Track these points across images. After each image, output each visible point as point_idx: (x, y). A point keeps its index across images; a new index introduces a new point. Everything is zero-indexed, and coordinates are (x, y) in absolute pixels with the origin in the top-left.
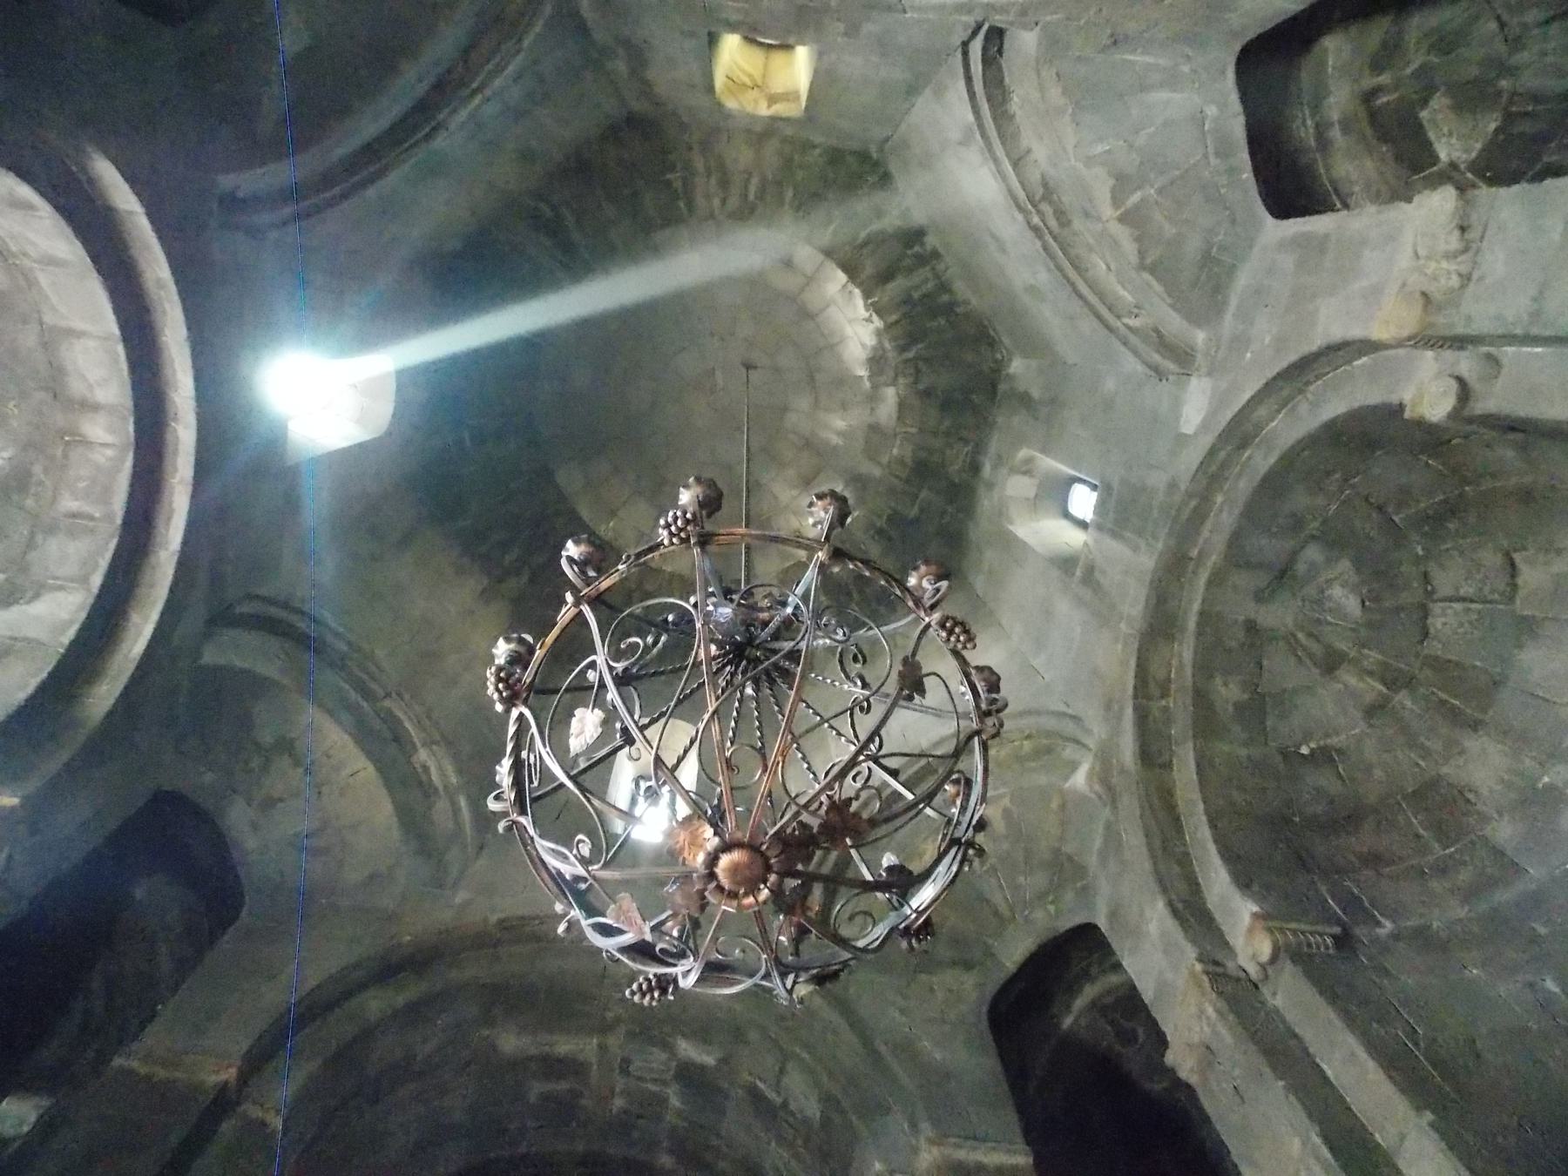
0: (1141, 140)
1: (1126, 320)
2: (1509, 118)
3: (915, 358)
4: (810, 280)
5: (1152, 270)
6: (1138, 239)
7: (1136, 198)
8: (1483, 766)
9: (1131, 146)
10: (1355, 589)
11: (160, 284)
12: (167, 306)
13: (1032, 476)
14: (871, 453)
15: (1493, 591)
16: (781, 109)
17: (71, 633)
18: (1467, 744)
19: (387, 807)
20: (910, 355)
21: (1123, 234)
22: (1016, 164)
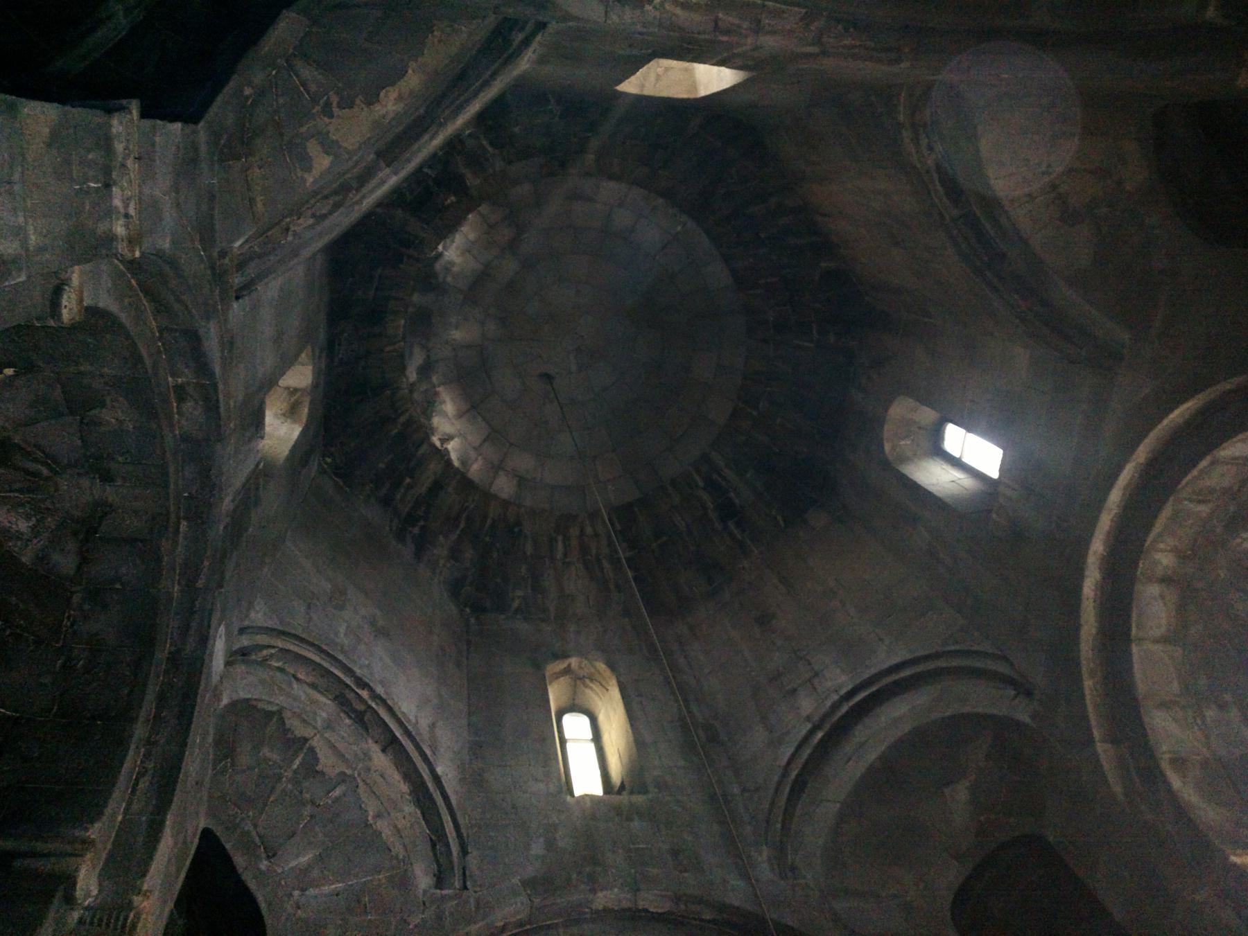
0: (307, 811)
1: (273, 651)
5: (270, 715)
9: (313, 802)
11: (1092, 674)
12: (1090, 654)
13: (287, 388)
16: (560, 666)
17: (1240, 436)
19: (984, 145)
20: (402, 419)
21: (300, 730)
22: (394, 740)
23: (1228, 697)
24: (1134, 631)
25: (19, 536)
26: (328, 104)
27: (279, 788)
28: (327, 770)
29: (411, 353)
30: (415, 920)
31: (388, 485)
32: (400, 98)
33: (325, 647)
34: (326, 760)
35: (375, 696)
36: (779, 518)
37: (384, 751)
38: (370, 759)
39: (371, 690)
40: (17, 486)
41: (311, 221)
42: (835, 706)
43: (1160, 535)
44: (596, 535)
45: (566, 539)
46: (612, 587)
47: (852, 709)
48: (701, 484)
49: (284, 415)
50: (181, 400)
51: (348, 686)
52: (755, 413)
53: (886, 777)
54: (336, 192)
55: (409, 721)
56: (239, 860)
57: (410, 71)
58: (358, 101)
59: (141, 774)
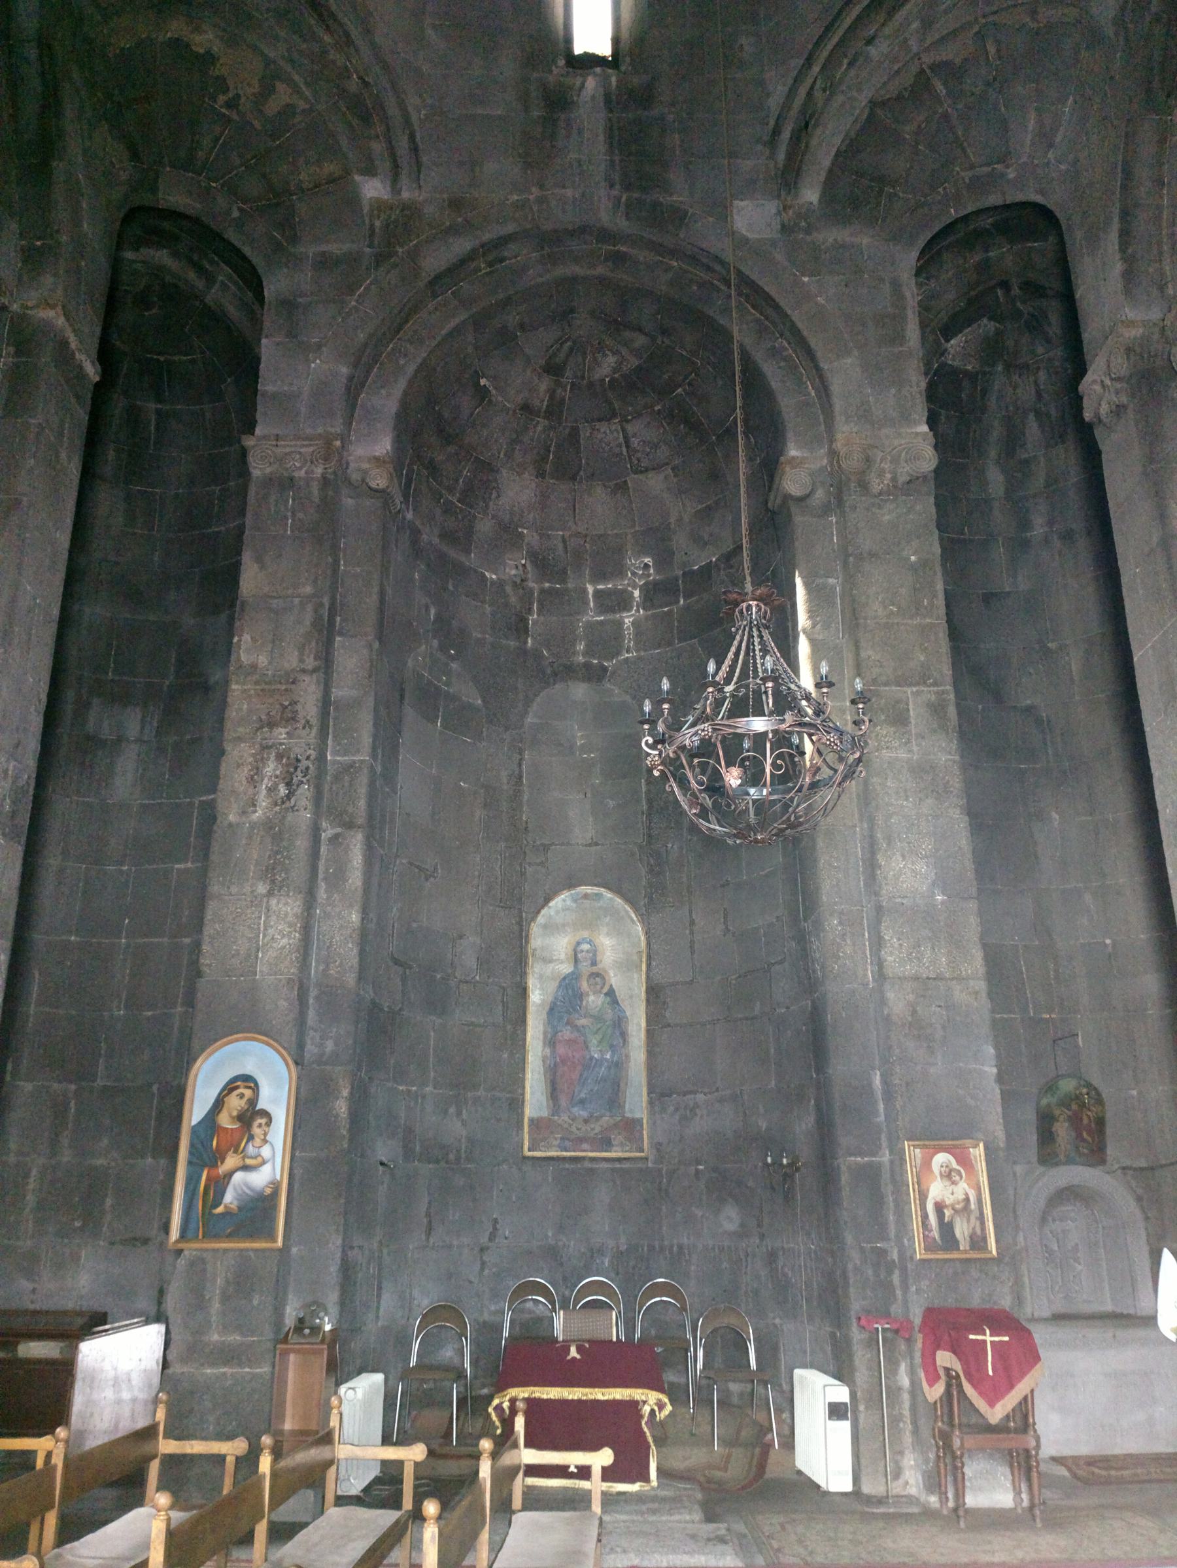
2: (972, 377)
6: (899, 98)
7: (940, 88)
8: (517, 491)
9: (988, 84)
10: (615, 371)
15: (639, 460)
18: (526, 475)
21: (908, 79)
26: (229, 105)
32: (197, 30)
34: (950, 53)
40: (580, 359)
50: (502, 260)
54: (320, 15)
57: (169, 35)
58: (217, 73)
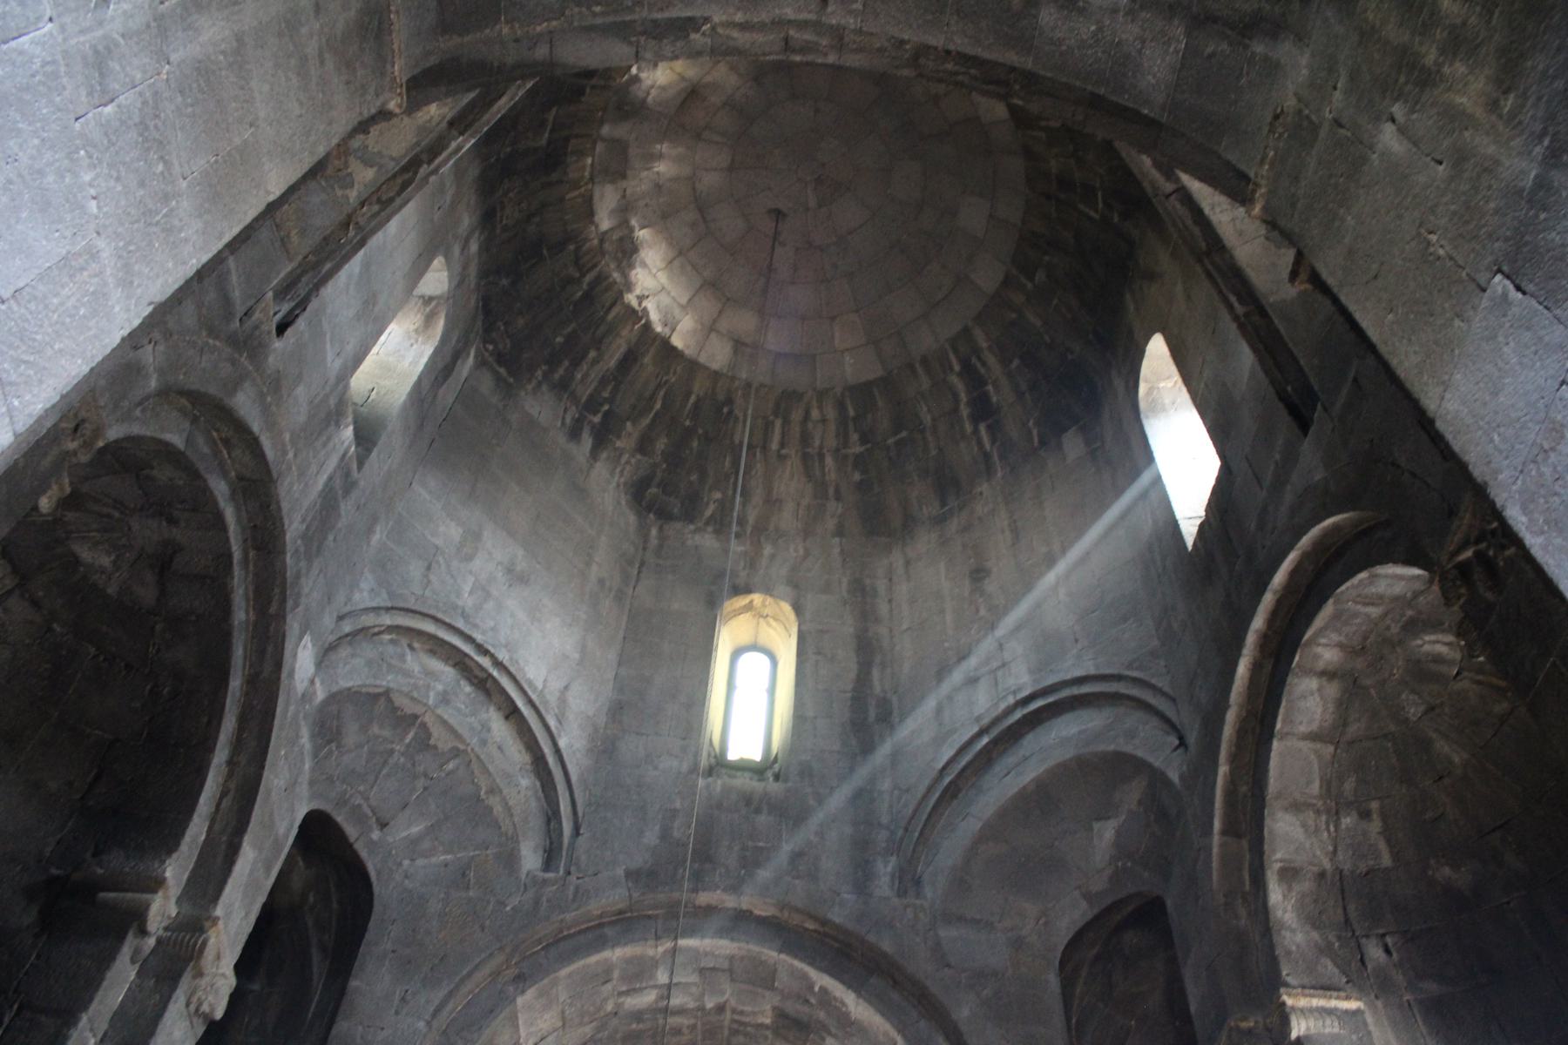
0: (420, 783)
3: (583, 275)
4: (710, 328)
5: (376, 696)
6: (395, 709)
9: (426, 775)
13: (422, 297)
14: (620, 149)
16: (742, 601)
20: (588, 278)
21: (409, 708)
23: (1375, 805)
24: (1278, 726)
25: (102, 570)
27: (391, 761)
28: (440, 745)
29: (602, 196)
30: (514, 901)
31: (566, 363)
33: (440, 616)
34: (438, 736)
35: (498, 664)
36: (1035, 432)
37: (507, 718)
38: (489, 730)
39: (492, 656)
40: (95, 526)
41: (376, 208)
42: (1009, 711)
43: (1321, 632)
44: (824, 421)
45: (786, 422)
46: (831, 491)
47: (1024, 716)
48: (957, 368)
49: (416, 331)
51: (466, 655)
52: (1029, 285)
53: (1040, 800)
55: (535, 690)
56: (351, 831)
59: (224, 794)
